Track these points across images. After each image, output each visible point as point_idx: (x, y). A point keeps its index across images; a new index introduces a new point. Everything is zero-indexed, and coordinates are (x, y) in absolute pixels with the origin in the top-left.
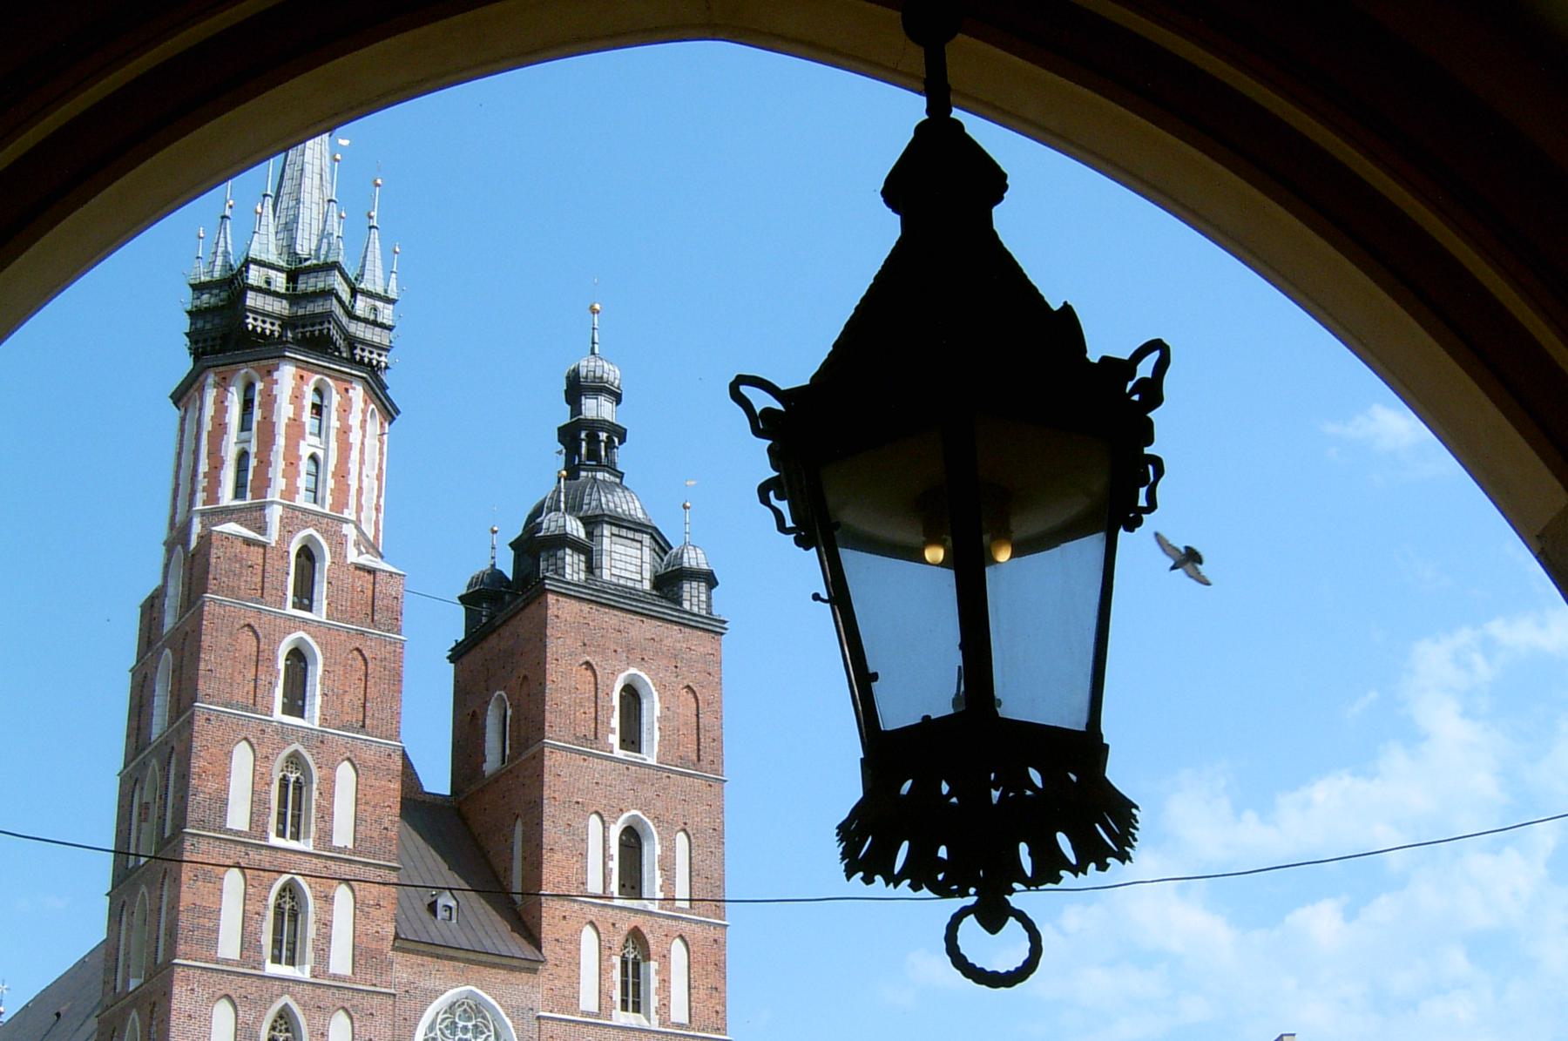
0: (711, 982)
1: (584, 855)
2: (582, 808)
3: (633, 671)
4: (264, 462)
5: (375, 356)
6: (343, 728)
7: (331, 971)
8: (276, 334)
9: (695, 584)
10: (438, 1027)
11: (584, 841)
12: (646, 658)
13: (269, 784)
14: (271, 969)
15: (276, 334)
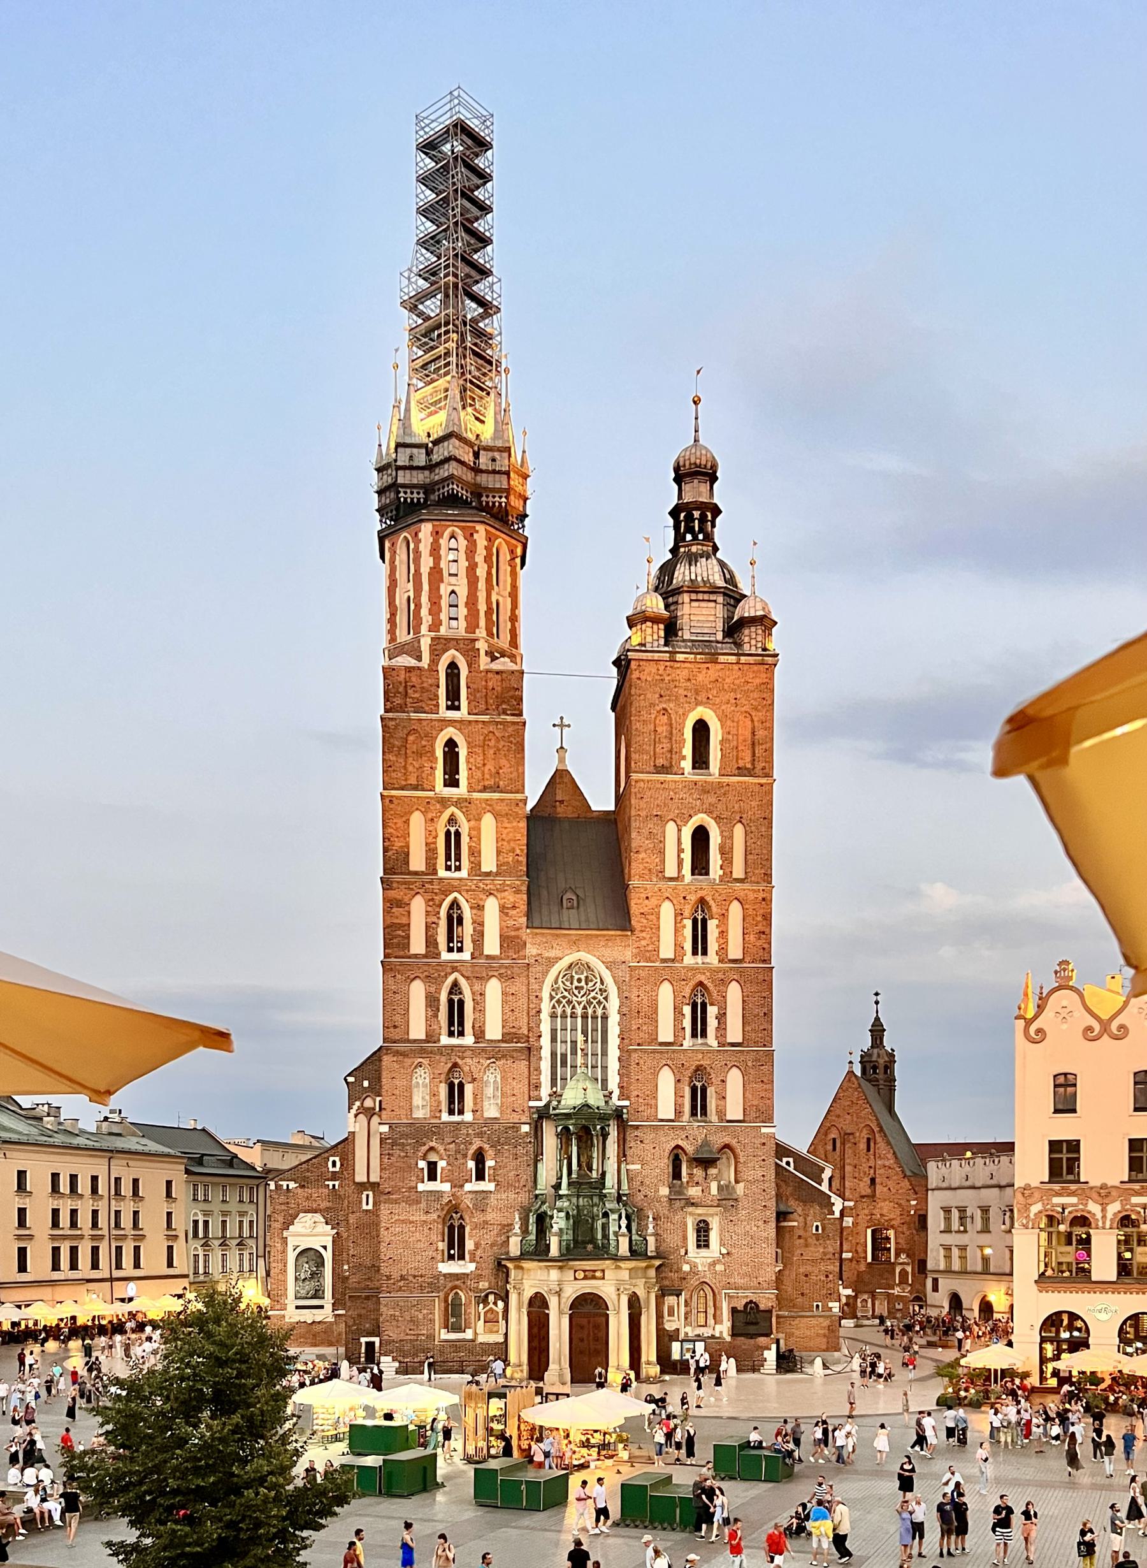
0: (760, 928)
1: (662, 852)
2: (662, 820)
3: (700, 709)
4: (418, 606)
5: (497, 499)
6: (485, 789)
7: (486, 952)
8: (422, 500)
9: (753, 629)
10: (560, 980)
11: (663, 842)
12: (711, 697)
13: (435, 837)
14: (445, 956)
15: (422, 500)
